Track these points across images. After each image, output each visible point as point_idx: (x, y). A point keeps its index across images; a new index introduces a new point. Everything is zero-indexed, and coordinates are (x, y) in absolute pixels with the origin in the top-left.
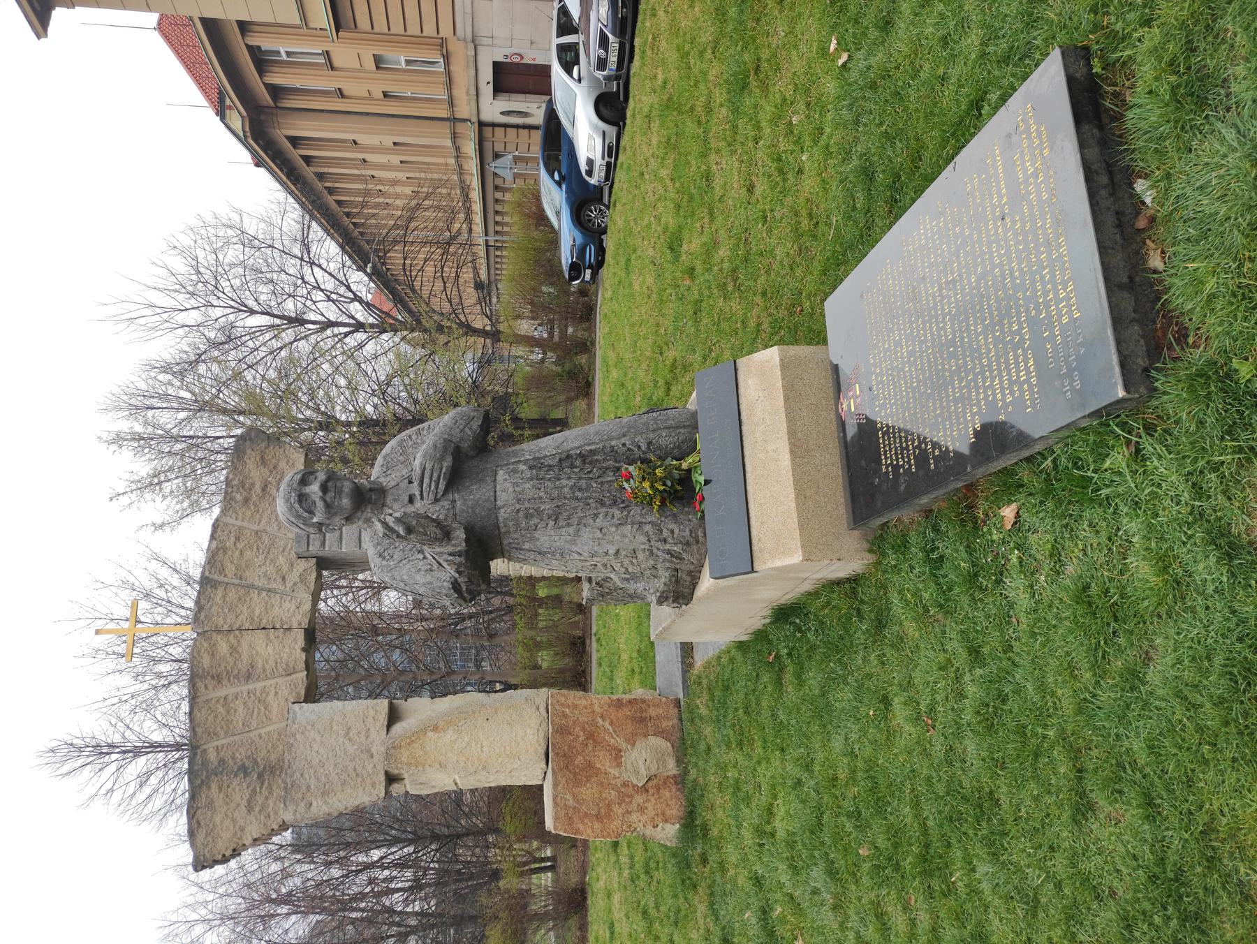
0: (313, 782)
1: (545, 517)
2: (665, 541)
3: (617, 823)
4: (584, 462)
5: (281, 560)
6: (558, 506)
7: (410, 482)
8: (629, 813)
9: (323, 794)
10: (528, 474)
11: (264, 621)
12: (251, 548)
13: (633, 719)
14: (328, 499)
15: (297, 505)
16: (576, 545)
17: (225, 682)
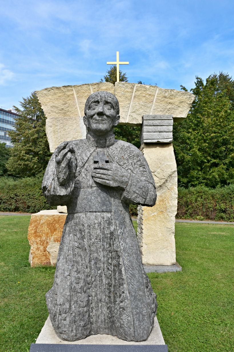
0: (58, 127)
2: (60, 315)
3: (33, 239)
4: (115, 266)
6: (86, 250)
7: (107, 162)
8: (37, 243)
9: (54, 131)
10: (107, 232)
14: (94, 117)
15: (93, 100)
16: (63, 259)
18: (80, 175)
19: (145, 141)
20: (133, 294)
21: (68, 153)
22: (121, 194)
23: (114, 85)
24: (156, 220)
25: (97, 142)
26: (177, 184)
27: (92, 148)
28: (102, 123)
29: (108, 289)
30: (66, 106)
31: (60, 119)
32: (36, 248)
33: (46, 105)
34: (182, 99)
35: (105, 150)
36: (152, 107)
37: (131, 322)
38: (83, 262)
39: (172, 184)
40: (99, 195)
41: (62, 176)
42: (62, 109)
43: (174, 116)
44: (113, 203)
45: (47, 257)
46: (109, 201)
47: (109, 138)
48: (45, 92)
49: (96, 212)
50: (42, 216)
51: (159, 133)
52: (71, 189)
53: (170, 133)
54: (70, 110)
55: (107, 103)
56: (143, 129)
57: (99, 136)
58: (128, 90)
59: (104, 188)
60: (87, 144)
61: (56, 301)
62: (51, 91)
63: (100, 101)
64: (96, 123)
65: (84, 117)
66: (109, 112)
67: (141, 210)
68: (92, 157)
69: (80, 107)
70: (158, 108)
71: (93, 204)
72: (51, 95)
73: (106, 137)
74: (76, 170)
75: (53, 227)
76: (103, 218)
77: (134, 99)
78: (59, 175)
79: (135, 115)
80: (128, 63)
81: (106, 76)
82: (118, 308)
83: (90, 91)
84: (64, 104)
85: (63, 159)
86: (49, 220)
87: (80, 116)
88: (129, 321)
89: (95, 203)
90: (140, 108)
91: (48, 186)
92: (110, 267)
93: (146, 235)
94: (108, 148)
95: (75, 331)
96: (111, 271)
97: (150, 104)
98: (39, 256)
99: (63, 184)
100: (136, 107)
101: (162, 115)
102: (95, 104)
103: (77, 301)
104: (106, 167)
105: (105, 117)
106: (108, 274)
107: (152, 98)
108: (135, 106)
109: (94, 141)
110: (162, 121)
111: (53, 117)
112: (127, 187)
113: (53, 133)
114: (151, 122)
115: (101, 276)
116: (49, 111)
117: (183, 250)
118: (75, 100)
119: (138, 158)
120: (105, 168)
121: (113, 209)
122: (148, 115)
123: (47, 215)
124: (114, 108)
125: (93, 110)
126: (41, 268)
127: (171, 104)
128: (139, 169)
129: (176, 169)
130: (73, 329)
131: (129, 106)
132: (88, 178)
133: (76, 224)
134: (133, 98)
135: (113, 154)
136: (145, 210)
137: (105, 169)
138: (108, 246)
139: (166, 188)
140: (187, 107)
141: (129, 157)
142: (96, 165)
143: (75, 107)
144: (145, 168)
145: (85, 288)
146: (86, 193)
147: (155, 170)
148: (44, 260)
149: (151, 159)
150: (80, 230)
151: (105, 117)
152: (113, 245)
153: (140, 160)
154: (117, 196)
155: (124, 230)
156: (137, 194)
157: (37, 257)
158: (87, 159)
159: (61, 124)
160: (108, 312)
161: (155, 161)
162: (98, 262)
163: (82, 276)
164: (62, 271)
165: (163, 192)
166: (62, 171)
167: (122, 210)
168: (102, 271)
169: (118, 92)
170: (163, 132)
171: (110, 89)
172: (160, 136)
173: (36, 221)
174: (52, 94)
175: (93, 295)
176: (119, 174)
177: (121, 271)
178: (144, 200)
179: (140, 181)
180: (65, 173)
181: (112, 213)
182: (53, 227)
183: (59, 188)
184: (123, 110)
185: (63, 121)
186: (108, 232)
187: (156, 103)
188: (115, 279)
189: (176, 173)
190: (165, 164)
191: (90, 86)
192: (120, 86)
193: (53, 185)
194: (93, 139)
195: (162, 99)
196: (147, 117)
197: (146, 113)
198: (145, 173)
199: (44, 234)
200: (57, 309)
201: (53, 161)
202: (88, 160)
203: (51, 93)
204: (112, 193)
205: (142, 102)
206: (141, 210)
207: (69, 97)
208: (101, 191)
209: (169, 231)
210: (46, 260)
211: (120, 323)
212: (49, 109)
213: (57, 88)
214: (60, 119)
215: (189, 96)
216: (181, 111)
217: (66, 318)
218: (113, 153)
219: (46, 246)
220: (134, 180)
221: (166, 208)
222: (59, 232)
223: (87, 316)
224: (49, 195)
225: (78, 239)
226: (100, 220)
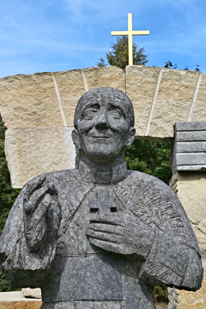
0: (27, 144)
5: (172, 115)
7: (113, 210)
9: (20, 151)
12: (180, 95)
14: (91, 131)
15: (89, 102)
18: (67, 233)
19: (179, 168)
21: (46, 196)
22: (139, 268)
23: (125, 71)
25: (95, 176)
27: (87, 186)
28: (104, 143)
30: (40, 107)
31: (30, 129)
33: (5, 106)
35: (110, 189)
36: (192, 108)
40: (99, 270)
42: (34, 113)
44: (124, 284)
46: (117, 280)
47: (117, 168)
48: (4, 83)
49: (93, 300)
52: (49, 259)
54: (48, 114)
55: (112, 107)
56: (175, 147)
57: (101, 164)
58: (149, 80)
60: (79, 178)
62: (14, 82)
63: (100, 104)
64: (94, 142)
65: (73, 131)
66: (117, 123)
68: (87, 202)
69: (65, 109)
70: (201, 110)
71: (88, 286)
72: (14, 88)
73: (112, 166)
74: (59, 225)
77: (158, 94)
78: (29, 234)
79: (160, 123)
80: (147, 32)
81: (109, 54)
83: (83, 81)
84: (38, 104)
85: (36, 207)
87: (66, 125)
89: (92, 284)
90: (169, 110)
91: (8, 252)
94: (115, 184)
100: (164, 108)
102: (92, 109)
104: (112, 220)
105: (109, 132)
107: (191, 92)
108: (162, 106)
109: (91, 172)
111: (18, 127)
112: (149, 255)
113: (17, 154)
116: (11, 116)
118: (57, 97)
119: (168, 203)
120: (109, 221)
122: (185, 123)
123: (4, 302)
124: (125, 116)
125: (89, 119)
128: (170, 222)
131: (149, 106)
135: (123, 195)
137: (110, 223)
141: (152, 200)
142: (94, 216)
144: (181, 221)
146: (76, 265)
147: (199, 220)
149: (192, 199)
151: (109, 132)
153: (171, 207)
154: (132, 272)
156: (167, 267)
158: (78, 204)
159: (32, 139)
161: (198, 204)
166: (34, 228)
167: (141, 296)
169: (131, 83)
171: (117, 78)
174: (16, 87)
176: (135, 232)
178: (180, 279)
179: (172, 244)
180: (39, 231)
181: (123, 303)
183: (28, 257)
184: (139, 115)
185: (35, 133)
187: (199, 102)
191: (83, 73)
192: (135, 73)
193: (17, 252)
194: (89, 170)
196: (183, 125)
197: (181, 119)
201: (19, 208)
202: (79, 206)
203: (14, 84)
204: (123, 266)
205: (172, 99)
207: (45, 92)
208: (103, 261)
212: (10, 113)
213: (25, 77)
214: (30, 129)
218: (124, 193)
220: (162, 242)
224: (10, 268)
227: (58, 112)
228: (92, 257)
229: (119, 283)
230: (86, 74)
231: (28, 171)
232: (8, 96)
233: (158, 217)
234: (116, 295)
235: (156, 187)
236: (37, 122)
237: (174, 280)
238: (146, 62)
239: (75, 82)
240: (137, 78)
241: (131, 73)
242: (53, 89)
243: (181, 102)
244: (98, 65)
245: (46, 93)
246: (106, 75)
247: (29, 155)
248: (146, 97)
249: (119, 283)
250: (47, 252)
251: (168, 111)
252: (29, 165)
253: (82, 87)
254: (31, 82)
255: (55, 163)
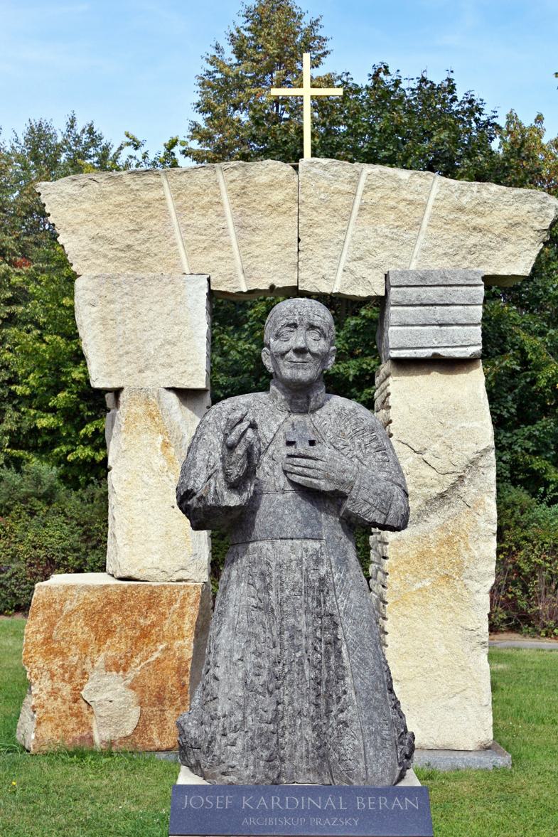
0: (117, 306)
1: (262, 595)
2: (224, 735)
4: (328, 643)
5: (383, 255)
6: (273, 611)
7: (312, 443)
8: (52, 676)
9: (104, 318)
10: (313, 576)
11: (308, 240)
13: (162, 688)
14: (288, 355)
15: (285, 321)
16: (228, 630)
17: (237, 201)
19: (394, 354)
20: (364, 696)
22: (340, 506)
24: (430, 602)
25: (291, 403)
26: (494, 489)
29: (315, 689)
30: (138, 236)
32: (50, 690)
34: (514, 214)
35: (307, 419)
37: (359, 750)
38: (268, 635)
39: (480, 489)
40: (298, 507)
41: (236, 472)
42: (129, 246)
43: (490, 271)
44: (324, 522)
45: (84, 719)
47: (315, 394)
49: (292, 539)
50: (68, 588)
51: (438, 328)
53: (472, 327)
54: (154, 249)
56: (386, 313)
57: (296, 391)
59: (309, 493)
61: (216, 710)
62: (90, 187)
67: (380, 574)
68: (282, 434)
72: (90, 199)
75: (105, 622)
76: (307, 551)
77: (358, 215)
79: (360, 269)
82: (334, 725)
83: (219, 188)
85: (239, 442)
86: (92, 602)
88: (355, 749)
90: (377, 245)
92: (318, 646)
93: (397, 650)
95: (252, 768)
96: (321, 654)
97: (410, 232)
98: (57, 715)
99: (236, 485)
100: (368, 241)
101: (449, 272)
102: (288, 329)
103: (256, 709)
105: (308, 356)
106: (314, 659)
109: (285, 400)
110: (449, 288)
113: (100, 324)
114: (412, 293)
115: (302, 664)
116: (85, 253)
117: (529, 721)
121: (325, 533)
123: (87, 586)
124: (325, 337)
126: (64, 754)
127: (481, 231)
128: (374, 457)
129: (492, 444)
130: (250, 763)
131: (342, 238)
132: (276, 473)
133: (253, 563)
134: (355, 212)
136: (393, 570)
138: (315, 605)
139: (460, 502)
140: (533, 241)
142: (292, 450)
143: (170, 241)
145: (271, 686)
147: (426, 446)
148: (73, 730)
150: (262, 574)
151: (308, 356)
152: (325, 603)
153: (376, 439)
155: (344, 575)
157: (51, 720)
158: (272, 436)
160: (315, 735)
161: (425, 418)
162: (297, 635)
163: (266, 663)
164: (227, 654)
165: (449, 513)
168: (304, 652)
169: (308, 193)
170: (452, 325)
171: (283, 184)
172: (443, 336)
173: (50, 606)
174: (93, 196)
175: (286, 702)
177: (341, 652)
178: (383, 516)
181: (323, 542)
182: (105, 622)
184: (322, 253)
185: (131, 286)
186: (315, 578)
187: (432, 231)
188: (329, 668)
189: (492, 454)
190: (456, 426)
192: (316, 174)
194: (283, 397)
195: (451, 217)
197: (399, 263)
198: (387, 464)
199: (73, 647)
200: (217, 726)
205: (384, 225)
206: (380, 574)
207: (149, 207)
209: (471, 639)
210: (79, 728)
211: (339, 753)
212: (83, 247)
214: (122, 279)
215: (537, 206)
216: (511, 254)
217: (236, 739)
219: (81, 685)
221: (460, 567)
222: (121, 638)
223: (275, 741)
225: (258, 591)
226: (300, 553)
227: (172, 245)
228: (291, 494)
229: (318, 522)
230: (225, 174)
231: (121, 356)
232: (79, 213)
233: (361, 451)
234: (316, 533)
235: (359, 416)
236: (134, 264)
237: (377, 518)
238: (325, 53)
239: (205, 190)
240: (319, 184)
241: (309, 175)
242: (163, 202)
243: (400, 232)
244: (207, 59)
245: (150, 210)
246: (262, 177)
247: (122, 327)
248: (335, 220)
249: (318, 522)
250: (246, 488)
251: (376, 247)
252: (121, 346)
253: (217, 200)
254: (121, 188)
255: (169, 343)
